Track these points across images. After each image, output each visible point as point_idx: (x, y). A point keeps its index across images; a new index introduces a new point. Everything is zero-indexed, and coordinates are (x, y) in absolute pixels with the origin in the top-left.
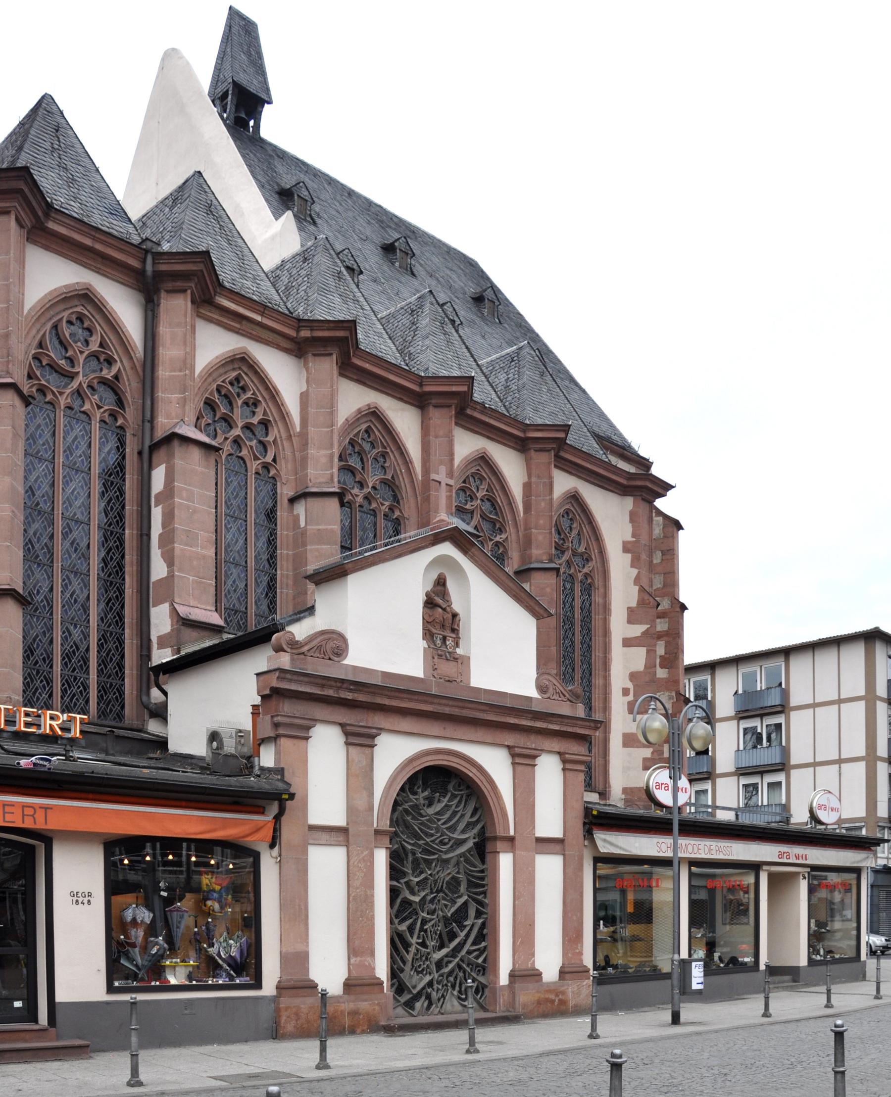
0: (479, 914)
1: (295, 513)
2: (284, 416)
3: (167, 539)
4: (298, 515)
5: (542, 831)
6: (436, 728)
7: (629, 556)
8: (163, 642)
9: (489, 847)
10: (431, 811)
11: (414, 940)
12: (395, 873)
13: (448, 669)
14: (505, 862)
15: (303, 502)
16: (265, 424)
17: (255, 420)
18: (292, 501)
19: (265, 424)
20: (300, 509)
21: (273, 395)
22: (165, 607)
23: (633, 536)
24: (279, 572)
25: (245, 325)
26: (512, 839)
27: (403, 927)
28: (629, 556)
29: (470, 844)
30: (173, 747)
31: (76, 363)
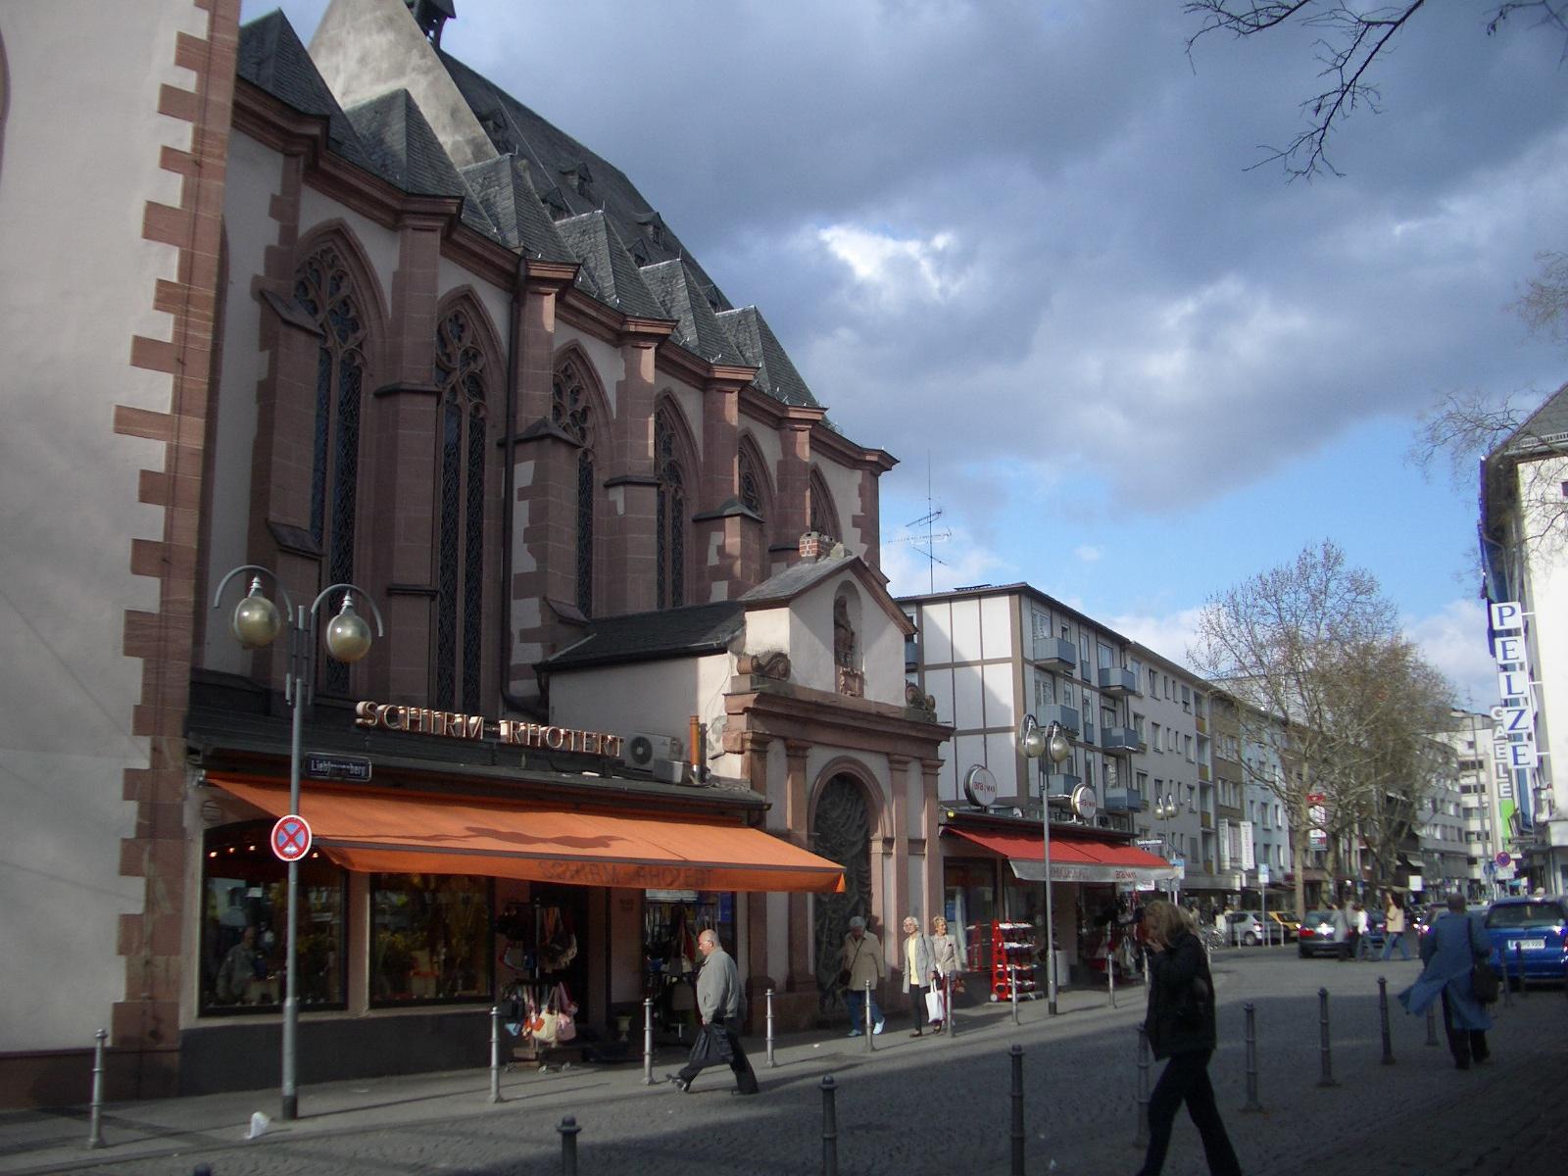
1: (611, 499)
2: (604, 404)
3: (531, 536)
4: (614, 504)
7: (859, 531)
8: (528, 636)
15: (621, 489)
16: (585, 410)
17: (579, 407)
18: (608, 486)
19: (585, 410)
20: (618, 496)
21: (596, 382)
22: (534, 603)
23: (862, 511)
24: (594, 557)
28: (859, 531)
31: (453, 358)
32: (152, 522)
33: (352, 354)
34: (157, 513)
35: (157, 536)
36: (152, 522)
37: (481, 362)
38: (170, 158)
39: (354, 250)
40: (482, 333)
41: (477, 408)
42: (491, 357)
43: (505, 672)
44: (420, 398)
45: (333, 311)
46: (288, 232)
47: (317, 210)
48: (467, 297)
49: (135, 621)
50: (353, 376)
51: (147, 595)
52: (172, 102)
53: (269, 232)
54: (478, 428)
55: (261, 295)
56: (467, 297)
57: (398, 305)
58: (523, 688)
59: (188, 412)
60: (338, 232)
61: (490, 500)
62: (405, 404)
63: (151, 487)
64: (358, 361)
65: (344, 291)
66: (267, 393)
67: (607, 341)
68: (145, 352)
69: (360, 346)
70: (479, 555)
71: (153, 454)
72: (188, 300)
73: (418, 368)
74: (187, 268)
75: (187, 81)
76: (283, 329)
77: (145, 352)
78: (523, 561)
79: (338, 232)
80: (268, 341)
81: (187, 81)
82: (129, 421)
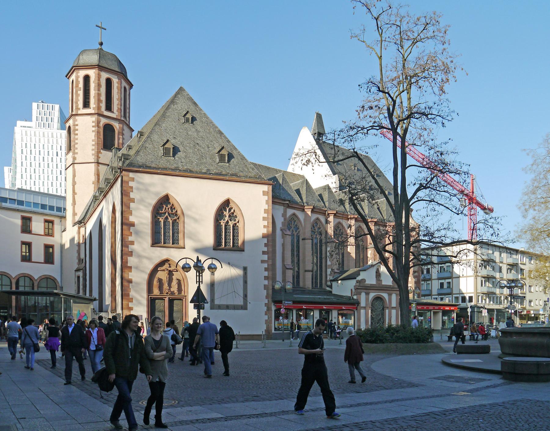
0: (383, 319)
5: (393, 306)
6: (377, 291)
9: (384, 308)
10: (376, 303)
11: (374, 323)
12: (371, 313)
13: (379, 282)
14: (387, 311)
25: (340, 217)
26: (388, 307)
27: (372, 321)
29: (382, 308)
30: (333, 293)
32: (266, 274)
33: (298, 233)
34: (267, 272)
35: (267, 275)
36: (266, 274)
37: (321, 229)
38: (264, 226)
39: (297, 216)
40: (321, 224)
41: (321, 237)
42: (323, 228)
43: (326, 281)
44: (308, 240)
45: (294, 227)
46: (285, 219)
47: (290, 212)
48: (318, 219)
49: (265, 285)
50: (298, 237)
51: (266, 282)
52: (264, 219)
53: (282, 219)
54: (321, 241)
55: (281, 230)
56: (318, 219)
57: (305, 225)
58: (329, 283)
59: (270, 259)
60: (294, 214)
61: (324, 252)
62: (306, 241)
63: (266, 269)
64: (299, 234)
65: (296, 224)
66: (283, 245)
67: (346, 220)
68: (264, 253)
69: (299, 232)
70: (322, 262)
71: (266, 265)
72: (268, 245)
73: (308, 234)
74: (268, 241)
75: (266, 215)
76: (285, 235)
77: (264, 253)
78: (329, 263)
79: (294, 214)
80: (283, 237)
81: (266, 215)
82: (263, 262)
